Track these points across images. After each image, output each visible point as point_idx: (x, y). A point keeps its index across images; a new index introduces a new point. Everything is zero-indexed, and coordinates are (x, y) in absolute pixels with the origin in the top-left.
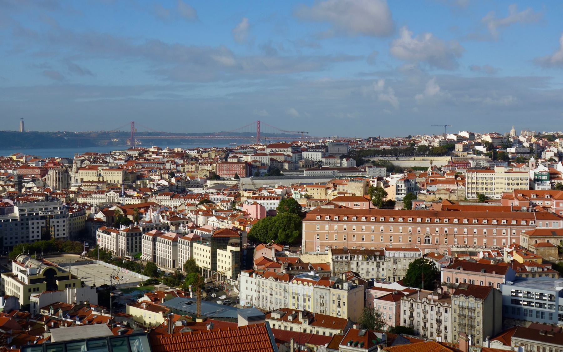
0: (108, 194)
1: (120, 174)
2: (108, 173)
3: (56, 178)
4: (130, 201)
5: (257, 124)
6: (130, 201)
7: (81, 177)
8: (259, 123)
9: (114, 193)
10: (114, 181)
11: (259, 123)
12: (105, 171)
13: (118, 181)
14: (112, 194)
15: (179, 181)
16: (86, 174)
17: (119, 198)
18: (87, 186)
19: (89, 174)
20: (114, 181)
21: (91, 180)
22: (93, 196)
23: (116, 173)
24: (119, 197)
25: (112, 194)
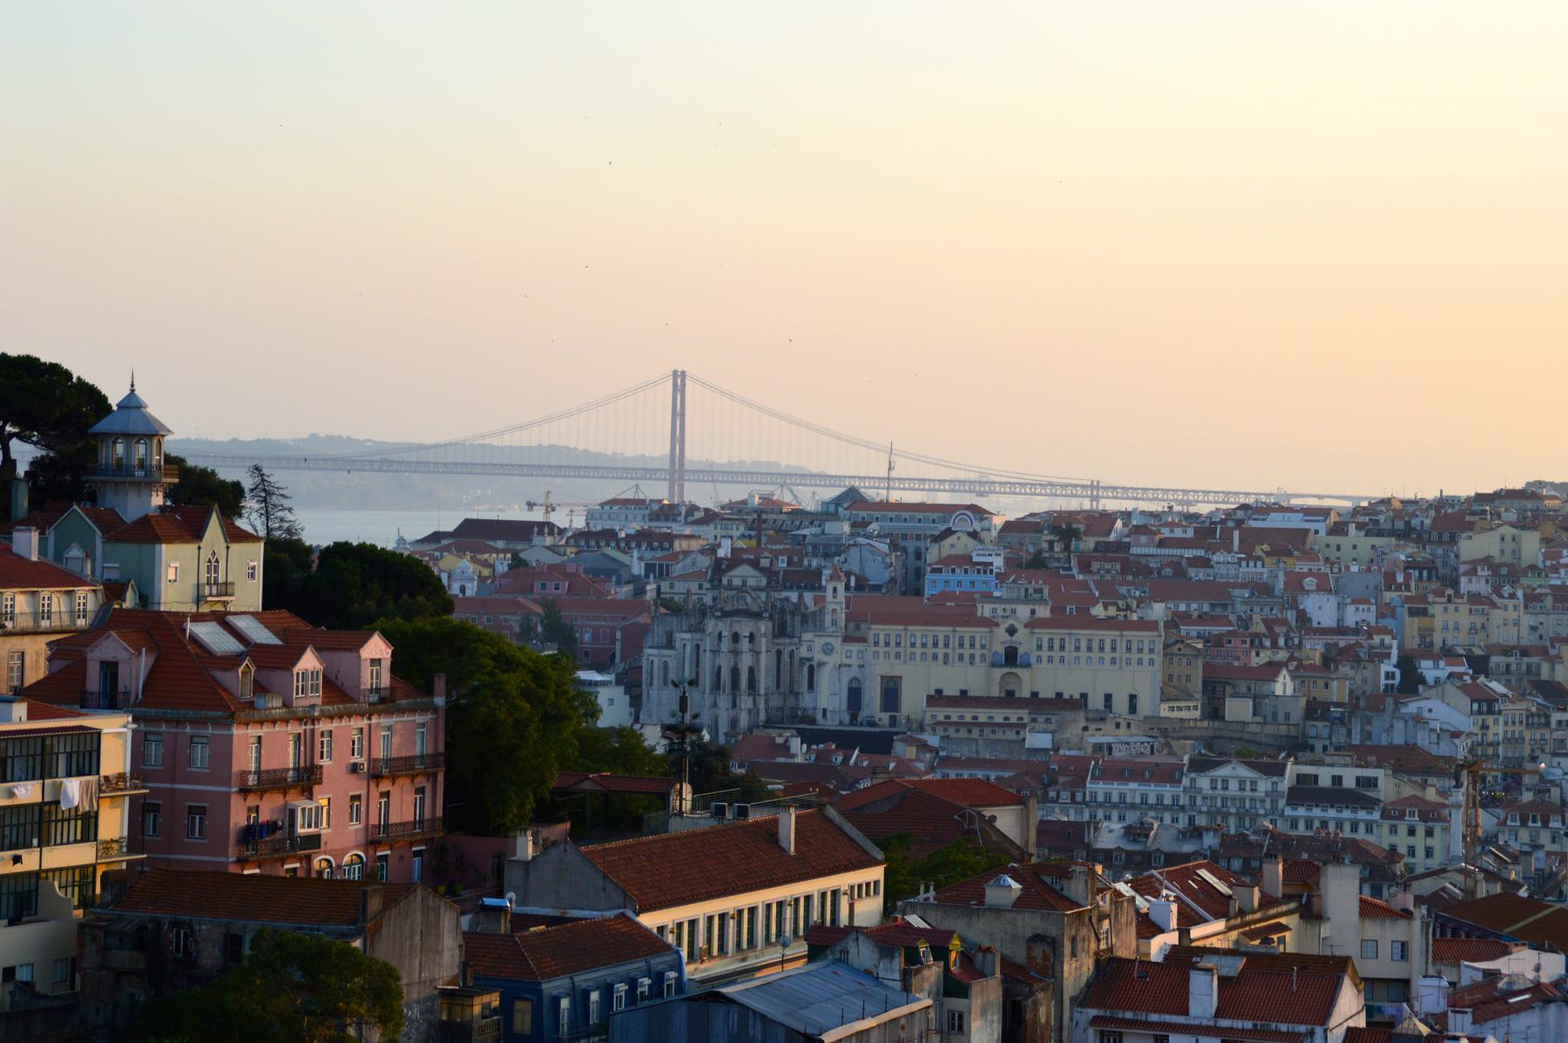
0: (1204, 782)
1: (1146, 657)
2: (1070, 646)
3: (735, 672)
4: (1369, 830)
5: (670, 384)
6: (1369, 830)
7: (882, 667)
8: (679, 381)
9: (1245, 772)
10: (1108, 698)
11: (679, 381)
12: (1045, 634)
13: (1133, 698)
14: (1234, 785)
15: (1491, 712)
16: (918, 651)
17: (1289, 812)
18: (969, 726)
19: (941, 651)
20: (1108, 698)
21: (952, 690)
22: (1094, 794)
23: (1122, 646)
24: (1282, 802)
25: (1234, 785)
